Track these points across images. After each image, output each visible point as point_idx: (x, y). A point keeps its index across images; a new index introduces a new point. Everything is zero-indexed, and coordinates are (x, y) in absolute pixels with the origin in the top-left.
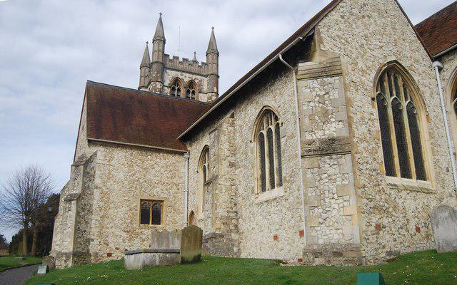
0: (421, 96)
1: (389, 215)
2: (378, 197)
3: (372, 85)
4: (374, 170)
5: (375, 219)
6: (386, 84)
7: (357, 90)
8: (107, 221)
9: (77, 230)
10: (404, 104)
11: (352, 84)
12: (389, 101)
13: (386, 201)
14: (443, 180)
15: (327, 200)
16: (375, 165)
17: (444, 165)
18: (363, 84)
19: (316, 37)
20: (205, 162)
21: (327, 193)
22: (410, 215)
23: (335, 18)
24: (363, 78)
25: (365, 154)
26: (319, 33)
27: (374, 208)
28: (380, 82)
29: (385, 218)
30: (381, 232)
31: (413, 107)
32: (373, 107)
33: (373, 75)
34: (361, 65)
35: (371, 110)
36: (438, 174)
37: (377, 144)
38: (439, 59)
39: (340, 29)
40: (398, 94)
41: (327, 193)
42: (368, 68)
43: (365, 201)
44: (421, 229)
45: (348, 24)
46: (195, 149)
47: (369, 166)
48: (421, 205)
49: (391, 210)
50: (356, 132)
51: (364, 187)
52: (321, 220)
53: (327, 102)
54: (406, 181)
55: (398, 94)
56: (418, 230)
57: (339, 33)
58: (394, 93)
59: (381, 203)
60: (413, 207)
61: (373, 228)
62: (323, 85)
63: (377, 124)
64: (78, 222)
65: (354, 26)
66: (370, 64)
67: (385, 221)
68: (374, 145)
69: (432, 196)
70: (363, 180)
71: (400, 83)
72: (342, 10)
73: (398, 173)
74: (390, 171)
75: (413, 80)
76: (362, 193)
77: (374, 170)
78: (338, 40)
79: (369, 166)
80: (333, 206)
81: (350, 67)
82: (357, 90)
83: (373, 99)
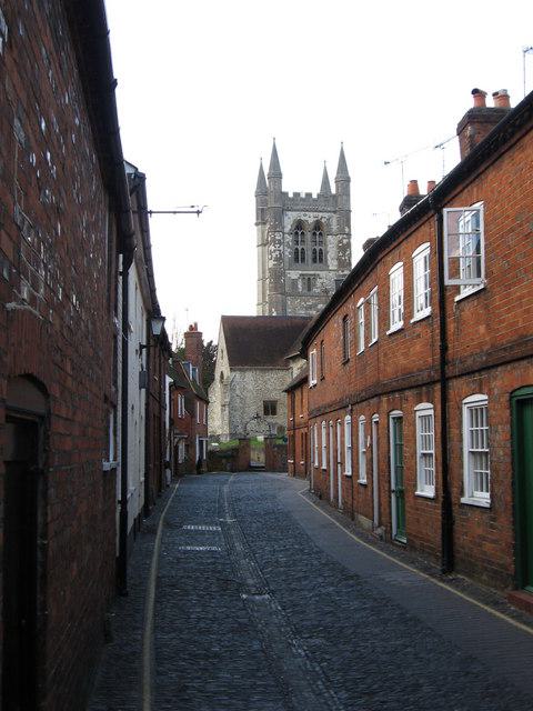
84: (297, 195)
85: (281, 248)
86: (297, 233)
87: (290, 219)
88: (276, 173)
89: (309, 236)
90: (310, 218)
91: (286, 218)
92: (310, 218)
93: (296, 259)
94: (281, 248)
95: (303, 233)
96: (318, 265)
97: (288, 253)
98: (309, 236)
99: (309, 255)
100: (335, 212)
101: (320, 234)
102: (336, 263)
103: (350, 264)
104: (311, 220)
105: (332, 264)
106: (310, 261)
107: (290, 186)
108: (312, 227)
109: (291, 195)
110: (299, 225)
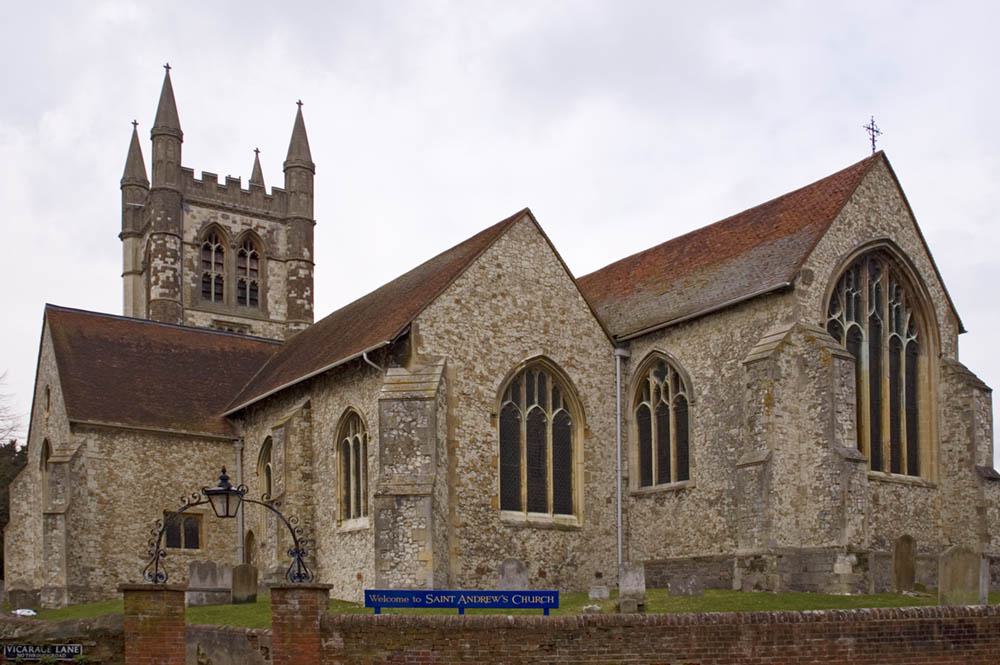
0: (581, 403)
1: (497, 555)
2: (484, 537)
3: (494, 395)
4: (483, 505)
5: (475, 563)
6: (523, 390)
7: (469, 405)
8: (112, 543)
9: (69, 557)
10: (550, 417)
11: (462, 397)
12: (525, 413)
13: (496, 541)
14: (598, 514)
15: (401, 544)
16: (485, 498)
17: (604, 494)
18: (480, 395)
19: (412, 336)
20: (269, 461)
21: (401, 536)
22: (532, 556)
23: (446, 304)
24: (481, 388)
25: (470, 487)
26: (417, 330)
27: (478, 549)
28: (511, 389)
29: (492, 561)
30: (484, 577)
31: (568, 418)
32: (493, 425)
33: (498, 382)
34: (480, 368)
35: (489, 428)
36: (588, 508)
37: (491, 473)
38: (626, 344)
39: (451, 321)
40: (542, 402)
41: (401, 536)
42: (491, 372)
43: (465, 541)
44: (548, 574)
45: (465, 311)
46: (254, 438)
47: (475, 501)
48: (553, 545)
49: (502, 551)
50: (461, 459)
51: (466, 525)
52: (392, 564)
53: (413, 432)
54: (535, 517)
55: (542, 402)
56: (542, 574)
57: (449, 327)
58: (536, 400)
59: (488, 544)
60: (539, 547)
61: (473, 572)
62: (409, 408)
63: (496, 448)
64: (69, 546)
65: (476, 313)
66: (495, 366)
67: (492, 564)
68: (487, 475)
69: (574, 534)
70: (464, 518)
71: (549, 386)
72: (459, 290)
73: (525, 507)
74: (510, 502)
75: (570, 381)
76: (462, 532)
77: (483, 505)
78: (446, 337)
79: (475, 501)
80: (407, 550)
81: (461, 375)
82: (469, 405)
83: (493, 416)
84: (210, 178)
85: (177, 266)
86: (207, 248)
87: (194, 221)
88: (168, 131)
89: (231, 255)
90: (236, 225)
91: (187, 217)
92: (236, 225)
93: (206, 293)
94: (177, 266)
95: (219, 251)
96: (248, 309)
97: (189, 279)
98: (231, 255)
99: (231, 289)
100: (284, 221)
101: (254, 257)
102: (283, 308)
103: (310, 314)
104: (237, 229)
105: (278, 311)
106: (234, 300)
107: (196, 158)
108: (238, 239)
109: (198, 176)
110: (212, 234)
